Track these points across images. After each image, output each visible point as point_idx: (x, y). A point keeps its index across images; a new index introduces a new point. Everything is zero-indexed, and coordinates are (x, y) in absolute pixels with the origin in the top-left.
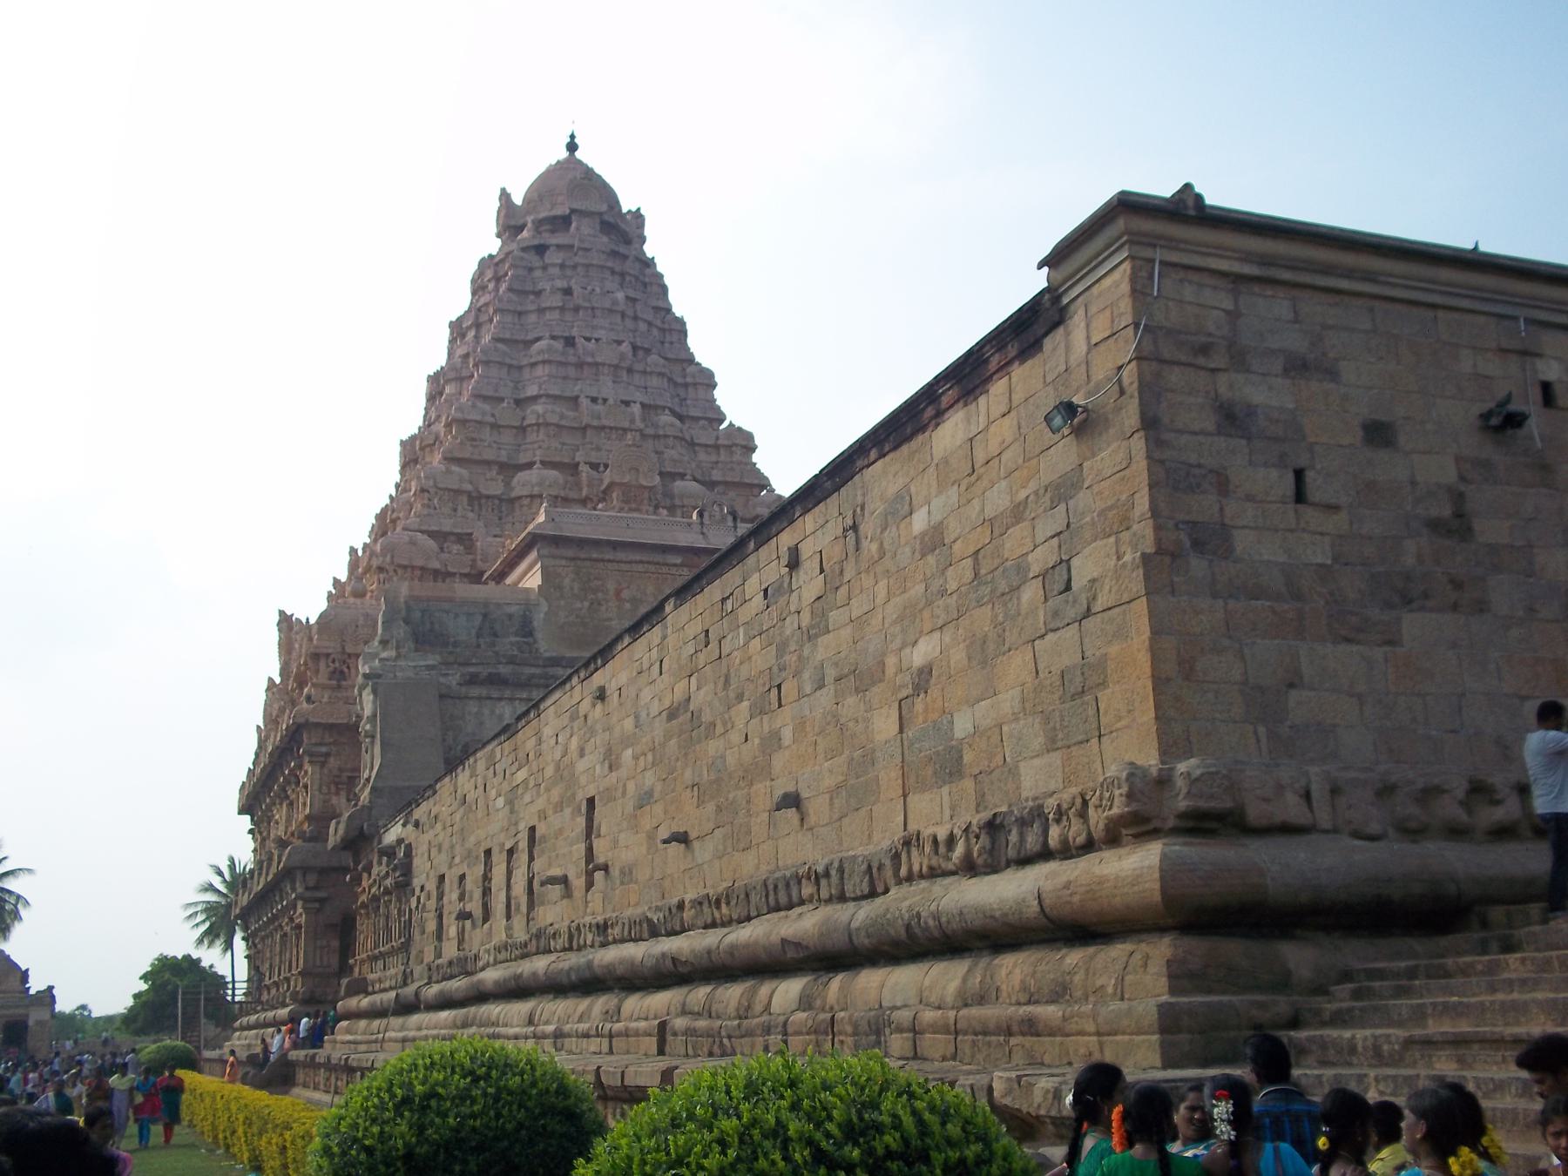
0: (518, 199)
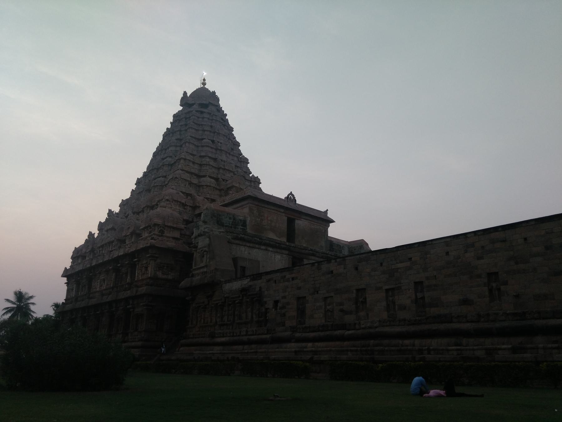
0: (188, 95)
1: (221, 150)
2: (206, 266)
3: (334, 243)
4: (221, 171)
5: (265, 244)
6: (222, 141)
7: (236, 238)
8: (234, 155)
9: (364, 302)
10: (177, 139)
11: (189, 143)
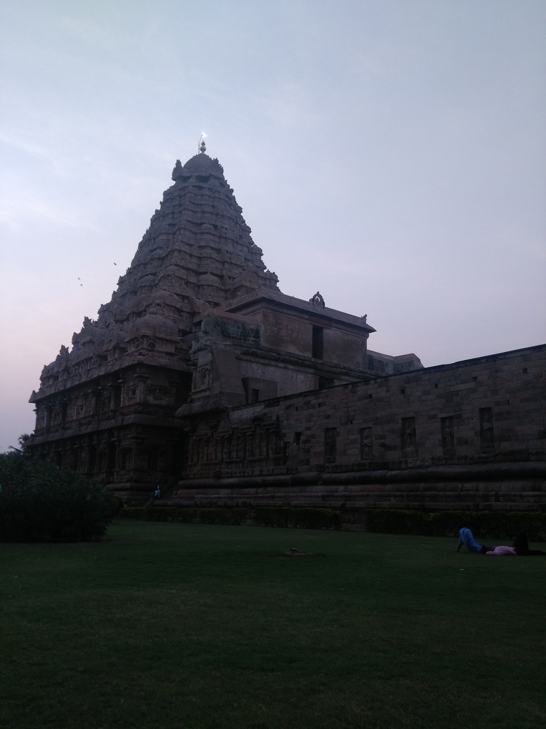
0: (183, 165)
1: (226, 238)
2: (209, 389)
3: (375, 359)
4: (227, 266)
5: (284, 361)
6: (227, 226)
7: (246, 353)
8: (243, 244)
9: (413, 434)
10: (169, 225)
11: (185, 229)
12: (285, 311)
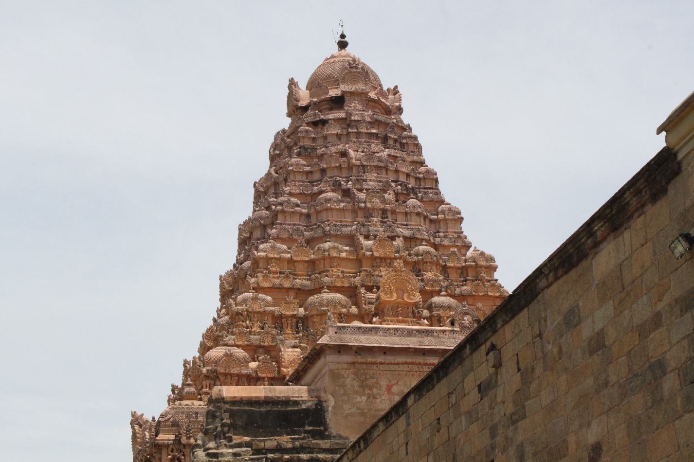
0: (303, 85)
12: (380, 359)
